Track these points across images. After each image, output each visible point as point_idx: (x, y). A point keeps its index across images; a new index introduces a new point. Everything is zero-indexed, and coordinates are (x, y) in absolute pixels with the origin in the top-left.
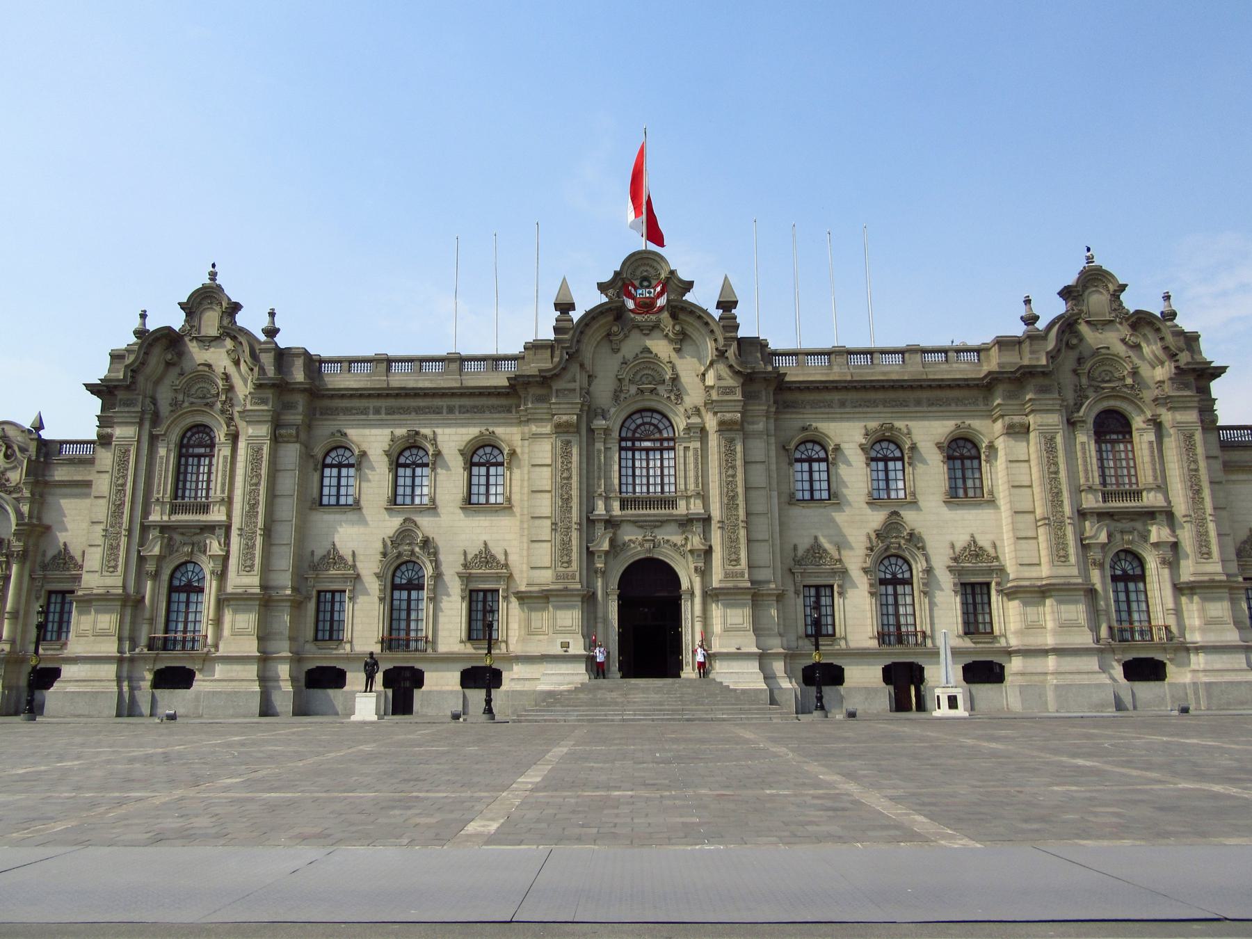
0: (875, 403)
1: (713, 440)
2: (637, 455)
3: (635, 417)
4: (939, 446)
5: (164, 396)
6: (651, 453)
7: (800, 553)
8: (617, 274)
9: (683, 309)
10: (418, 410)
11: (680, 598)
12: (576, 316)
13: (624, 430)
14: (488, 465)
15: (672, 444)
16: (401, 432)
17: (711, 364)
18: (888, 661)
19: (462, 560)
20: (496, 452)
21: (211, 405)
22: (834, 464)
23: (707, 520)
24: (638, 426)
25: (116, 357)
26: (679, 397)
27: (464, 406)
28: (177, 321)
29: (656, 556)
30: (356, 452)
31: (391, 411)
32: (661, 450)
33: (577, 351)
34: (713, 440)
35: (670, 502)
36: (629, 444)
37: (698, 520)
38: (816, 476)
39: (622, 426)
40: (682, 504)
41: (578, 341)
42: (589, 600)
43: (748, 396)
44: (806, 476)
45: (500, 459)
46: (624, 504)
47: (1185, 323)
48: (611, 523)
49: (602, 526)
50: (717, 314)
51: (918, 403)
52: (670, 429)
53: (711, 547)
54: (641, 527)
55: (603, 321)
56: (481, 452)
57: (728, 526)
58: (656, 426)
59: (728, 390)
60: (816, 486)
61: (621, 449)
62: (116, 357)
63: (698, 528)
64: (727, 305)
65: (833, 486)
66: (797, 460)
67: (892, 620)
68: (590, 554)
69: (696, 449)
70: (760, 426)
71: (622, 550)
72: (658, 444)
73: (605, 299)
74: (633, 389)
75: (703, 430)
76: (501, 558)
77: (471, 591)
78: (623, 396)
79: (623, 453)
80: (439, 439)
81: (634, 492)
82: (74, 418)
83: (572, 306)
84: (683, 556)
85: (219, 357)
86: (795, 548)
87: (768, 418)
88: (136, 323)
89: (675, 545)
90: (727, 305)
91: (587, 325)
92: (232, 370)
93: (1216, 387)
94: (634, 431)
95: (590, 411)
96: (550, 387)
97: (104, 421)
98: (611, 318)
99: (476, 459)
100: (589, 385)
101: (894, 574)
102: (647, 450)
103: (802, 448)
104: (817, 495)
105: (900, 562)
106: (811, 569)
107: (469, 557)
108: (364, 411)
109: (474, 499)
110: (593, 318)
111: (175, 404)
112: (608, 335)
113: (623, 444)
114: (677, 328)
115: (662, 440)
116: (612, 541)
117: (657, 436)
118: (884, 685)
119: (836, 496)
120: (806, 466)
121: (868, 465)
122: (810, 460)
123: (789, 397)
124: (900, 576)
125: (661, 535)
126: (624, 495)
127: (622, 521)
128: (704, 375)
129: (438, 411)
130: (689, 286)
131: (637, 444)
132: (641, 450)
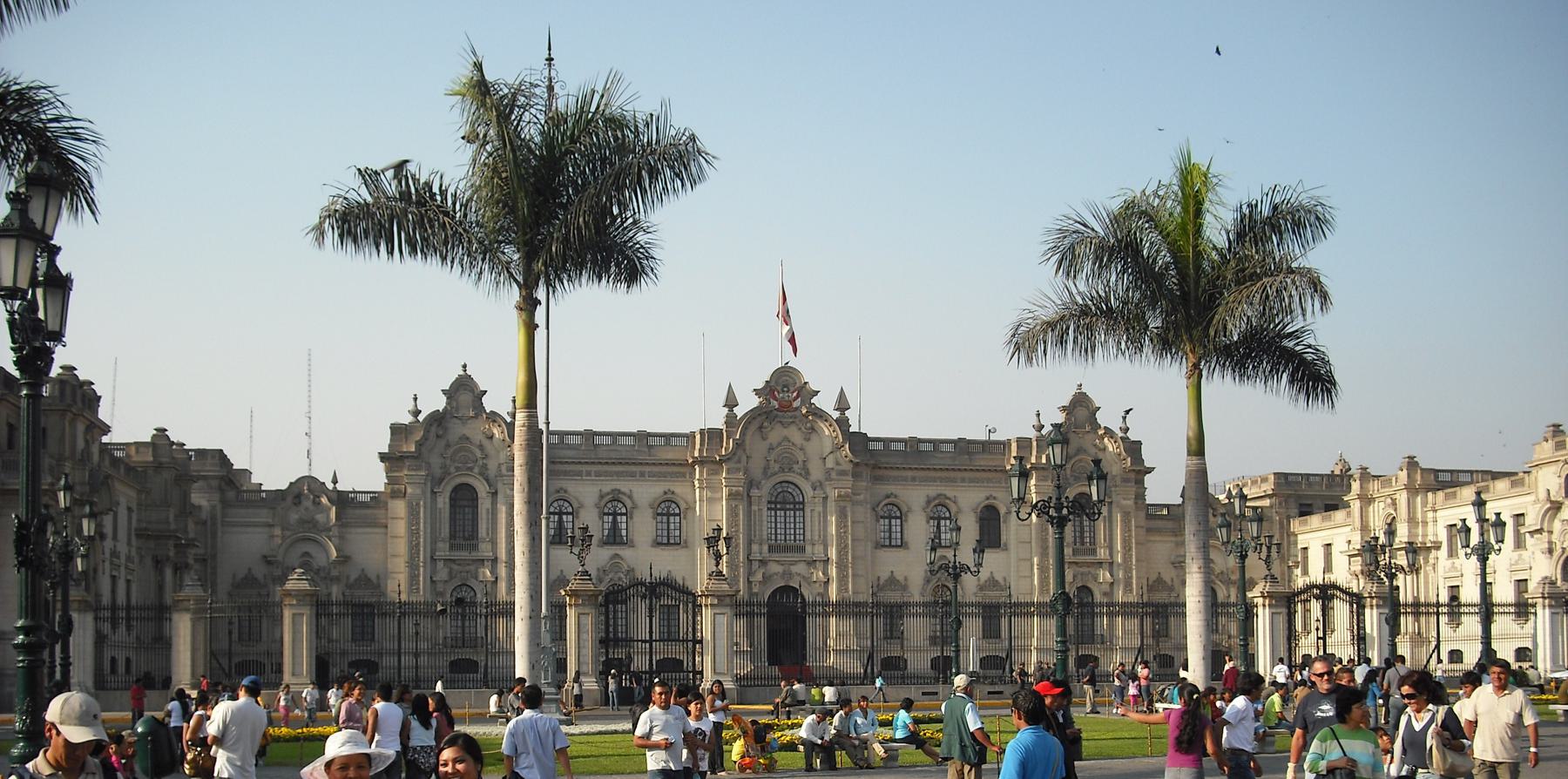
0: (934, 480)
1: (831, 505)
4: (974, 511)
5: (436, 461)
10: (618, 474)
12: (740, 412)
16: (607, 488)
21: (471, 469)
25: (397, 430)
26: (808, 473)
28: (440, 403)
30: (575, 505)
31: (598, 474)
32: (795, 510)
34: (831, 505)
35: (802, 549)
40: (808, 548)
43: (855, 475)
46: (771, 549)
47: (1132, 436)
48: (763, 562)
51: (963, 480)
57: (841, 566)
59: (843, 473)
62: (397, 430)
63: (820, 566)
64: (842, 405)
68: (750, 582)
75: (826, 498)
80: (635, 496)
82: (368, 477)
85: (475, 430)
88: (411, 406)
92: (486, 443)
93: (1147, 477)
95: (751, 484)
97: (391, 481)
108: (579, 474)
111: (444, 467)
112: (761, 427)
115: (795, 503)
122: (890, 518)
123: (881, 472)
125: (794, 569)
129: (632, 475)
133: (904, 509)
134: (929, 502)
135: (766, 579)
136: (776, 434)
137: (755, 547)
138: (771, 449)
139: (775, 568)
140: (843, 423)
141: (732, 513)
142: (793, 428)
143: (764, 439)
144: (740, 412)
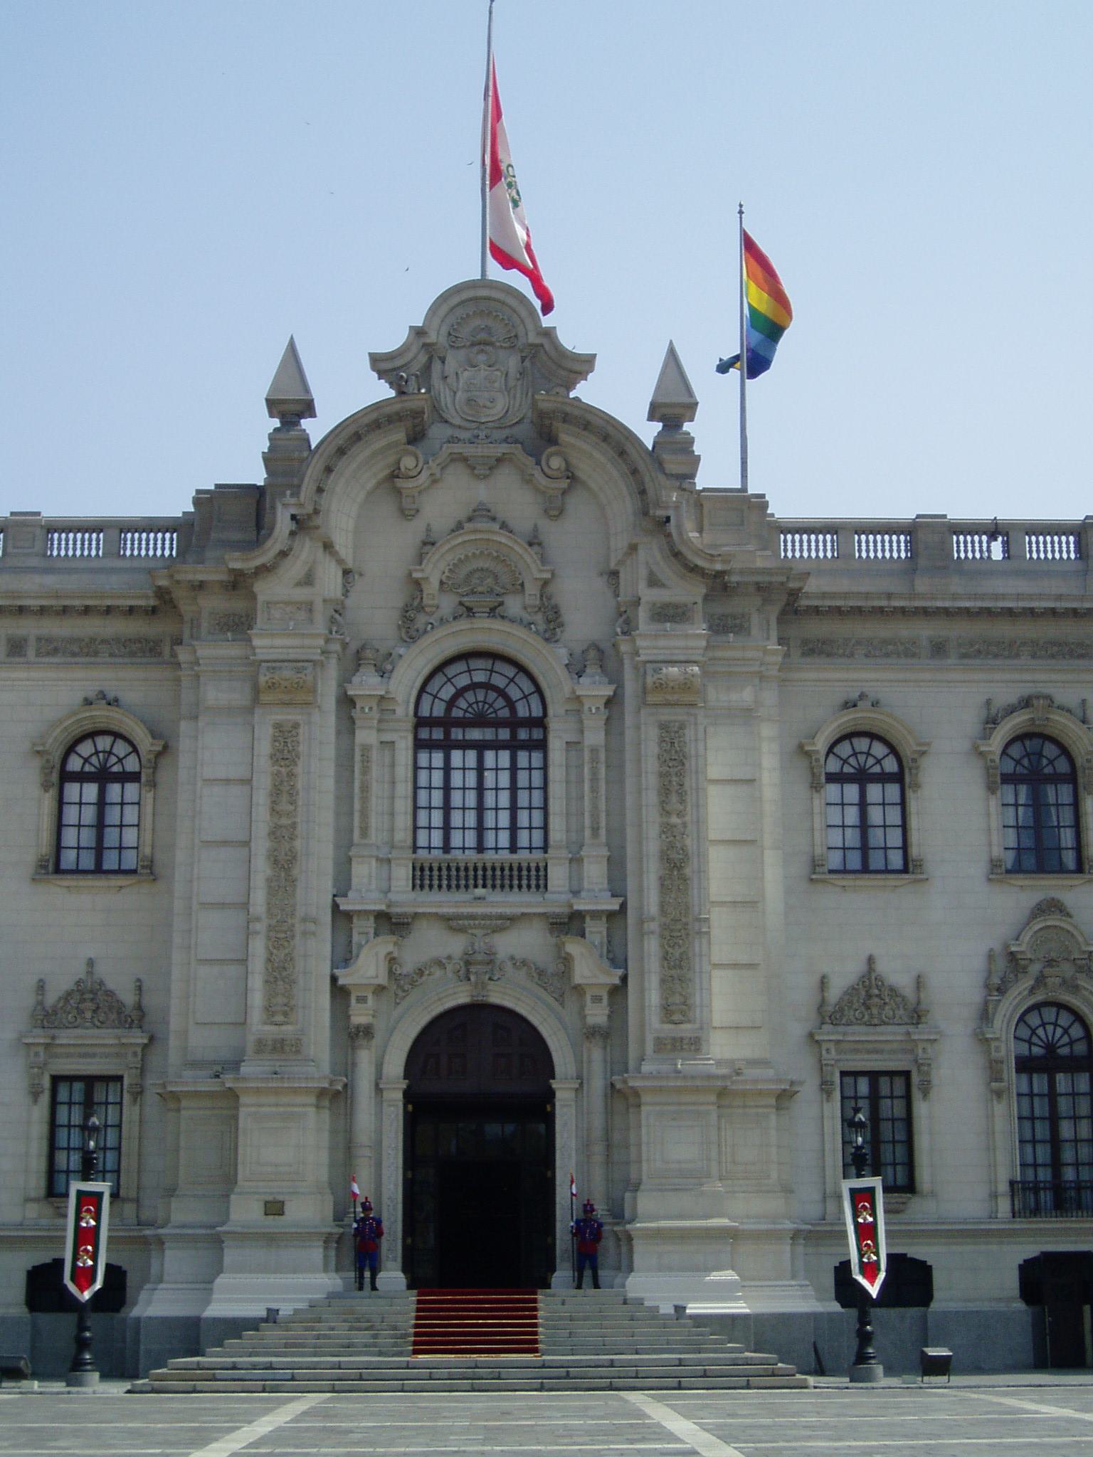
2: (456, 756)
3: (451, 671)
6: (489, 756)
7: (834, 994)
8: (418, 332)
9: (566, 418)
11: (551, 1095)
12: (316, 429)
13: (427, 700)
14: (103, 777)
15: (537, 734)
17: (633, 548)
18: (1031, 1250)
19: (30, 1000)
20: (121, 748)
22: (916, 786)
23: (616, 917)
24: (460, 693)
27: (49, 640)
29: (495, 999)
32: (513, 746)
33: (316, 512)
35: (536, 878)
36: (438, 734)
37: (595, 914)
38: (875, 815)
39: (422, 690)
40: (558, 875)
41: (320, 490)
42: (338, 1098)
43: (722, 626)
44: (852, 815)
45: (131, 765)
46: (423, 877)
48: (392, 923)
49: (370, 923)
50: (648, 433)
52: (535, 700)
53: (624, 979)
54: (462, 930)
55: (378, 442)
56: (86, 748)
58: (502, 693)
60: (876, 837)
61: (419, 745)
64: (673, 409)
65: (914, 837)
66: (831, 778)
67: (1043, 1153)
68: (339, 992)
69: (594, 750)
70: (746, 695)
71: (413, 984)
72: (504, 734)
73: (383, 391)
74: (447, 604)
76: (128, 998)
77: (56, 1080)
78: (421, 620)
79: (423, 758)
81: (446, 848)
83: (308, 409)
84: (560, 999)
86: (823, 983)
87: (762, 677)
89: (541, 973)
90: (673, 409)
91: (341, 452)
94: (451, 703)
96: (253, 597)
98: (399, 435)
99: (75, 764)
100: (346, 593)
101: (1050, 1047)
102: (480, 747)
103: (844, 749)
104: (876, 860)
105: (1065, 1019)
106: (859, 1033)
107: (51, 998)
109: (69, 858)
110: (357, 437)
112: (395, 475)
113: (424, 734)
114: (556, 463)
115: (514, 723)
116: (392, 960)
117: (505, 713)
118: (1020, 1305)
119: (919, 865)
120: (852, 791)
121: (991, 789)
122: (862, 778)
123: (816, 629)
124: (1064, 1051)
126: (422, 854)
127: (416, 915)
128: (614, 574)
130: (582, 366)
131: (457, 734)
132: (464, 745)
133: (907, 751)
134: (992, 722)
135: (399, 982)
136: (447, 499)
137: (363, 872)
138: (429, 543)
139: (432, 943)
140: (676, 449)
141: (286, 751)
142: (506, 480)
143: (407, 514)
144: (316, 429)
